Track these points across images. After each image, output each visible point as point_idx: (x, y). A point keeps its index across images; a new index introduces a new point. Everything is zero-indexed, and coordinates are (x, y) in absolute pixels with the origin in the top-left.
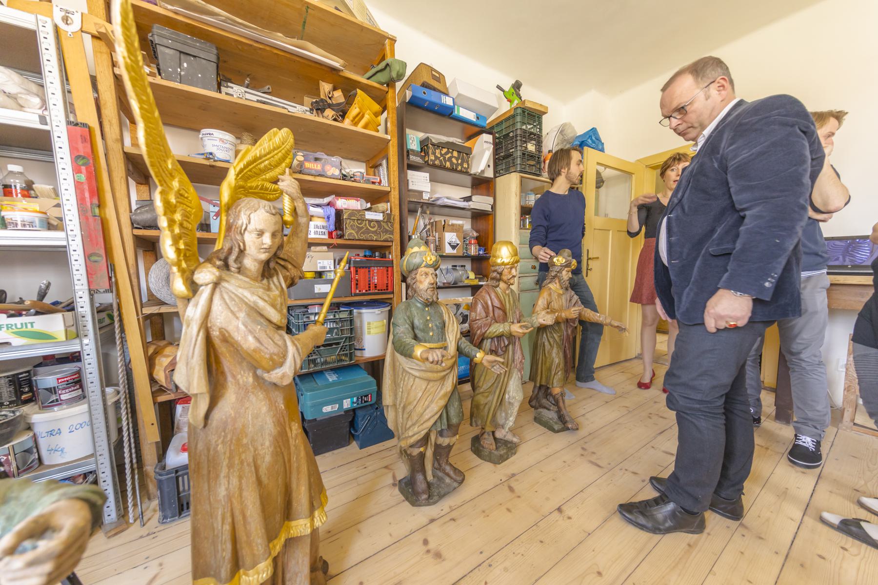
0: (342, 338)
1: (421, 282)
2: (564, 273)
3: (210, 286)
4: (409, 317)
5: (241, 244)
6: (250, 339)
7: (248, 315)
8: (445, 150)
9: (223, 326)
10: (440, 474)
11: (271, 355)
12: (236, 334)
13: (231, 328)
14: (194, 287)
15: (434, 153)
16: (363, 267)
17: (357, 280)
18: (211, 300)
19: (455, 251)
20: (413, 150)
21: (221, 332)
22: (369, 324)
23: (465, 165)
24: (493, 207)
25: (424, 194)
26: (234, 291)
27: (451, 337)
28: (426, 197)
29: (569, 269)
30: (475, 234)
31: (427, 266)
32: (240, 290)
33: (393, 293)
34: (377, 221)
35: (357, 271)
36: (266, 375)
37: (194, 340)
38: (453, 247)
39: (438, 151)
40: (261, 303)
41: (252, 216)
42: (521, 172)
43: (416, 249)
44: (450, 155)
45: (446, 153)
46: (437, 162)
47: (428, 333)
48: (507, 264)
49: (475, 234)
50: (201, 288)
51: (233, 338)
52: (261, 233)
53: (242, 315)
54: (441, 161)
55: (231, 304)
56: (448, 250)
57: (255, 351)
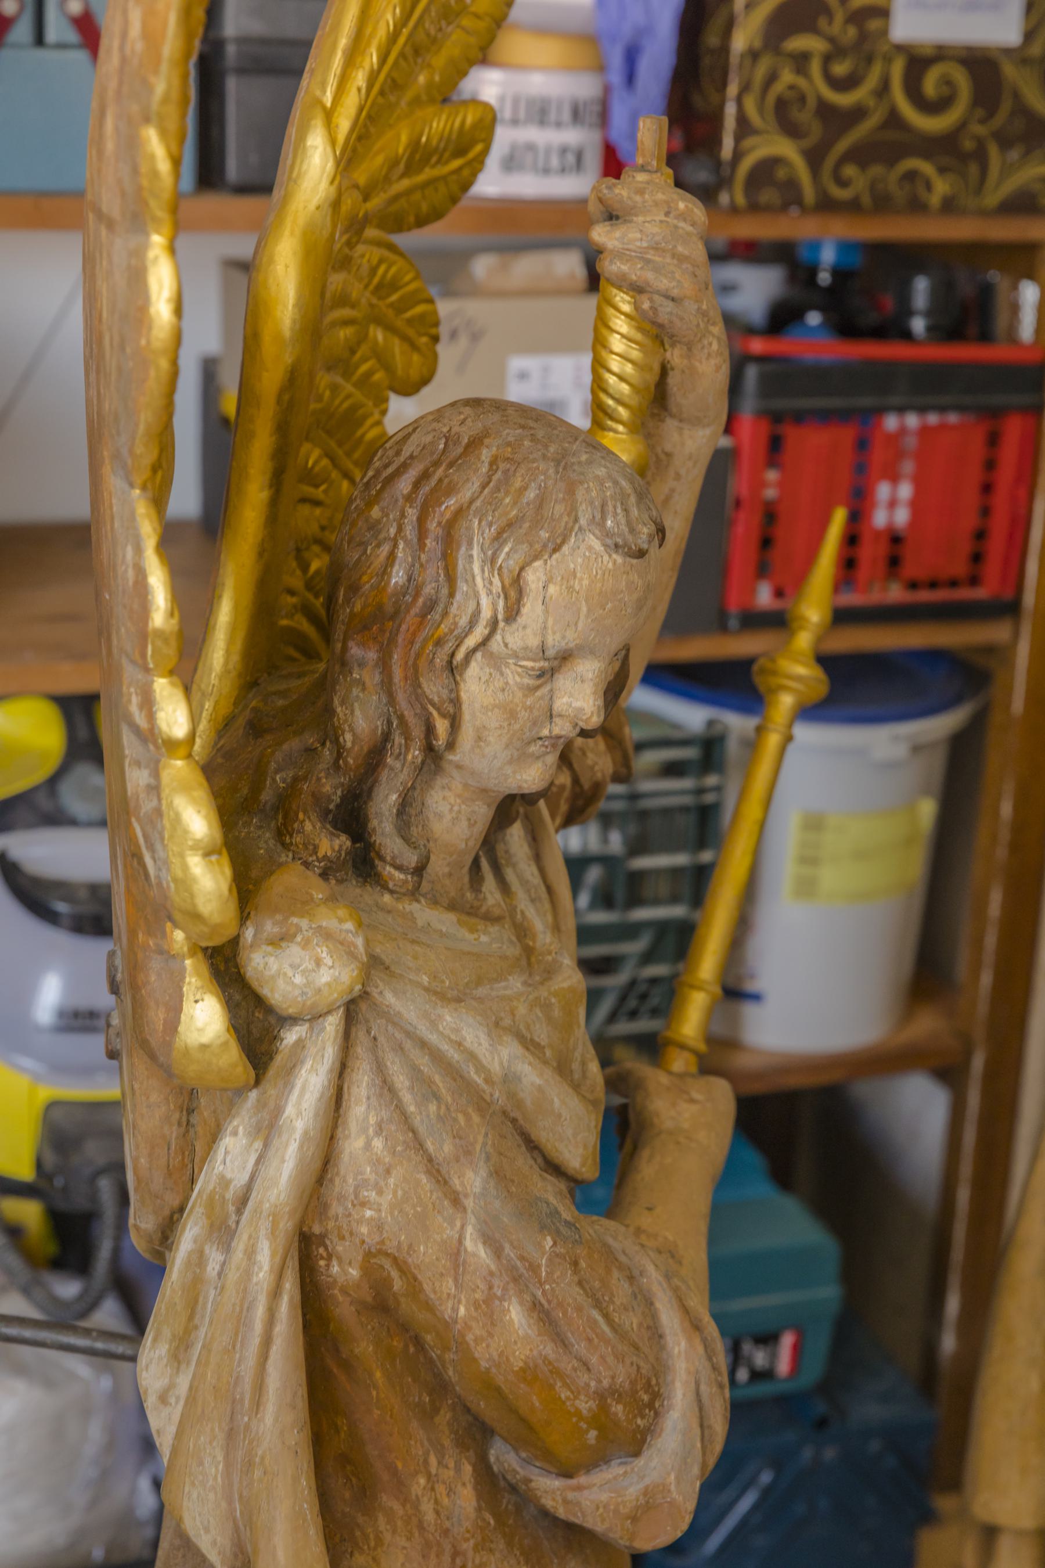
0: (631, 931)
3: (333, 1024)
5: (442, 726)
6: (516, 1314)
7: (498, 1174)
9: (391, 1247)
11: (601, 1397)
12: (448, 1285)
13: (425, 1255)
14: (258, 1030)
17: (770, 514)
18: (337, 1100)
21: (367, 1270)
22: (814, 824)
26: (423, 1030)
32: (448, 1018)
33: (1008, 608)
35: (775, 445)
36: (549, 1488)
37: (260, 1312)
40: (532, 1076)
41: (534, 577)
50: (291, 1036)
51: (428, 1307)
52: (554, 664)
53: (473, 1180)
55: (424, 1116)
57: (529, 1374)
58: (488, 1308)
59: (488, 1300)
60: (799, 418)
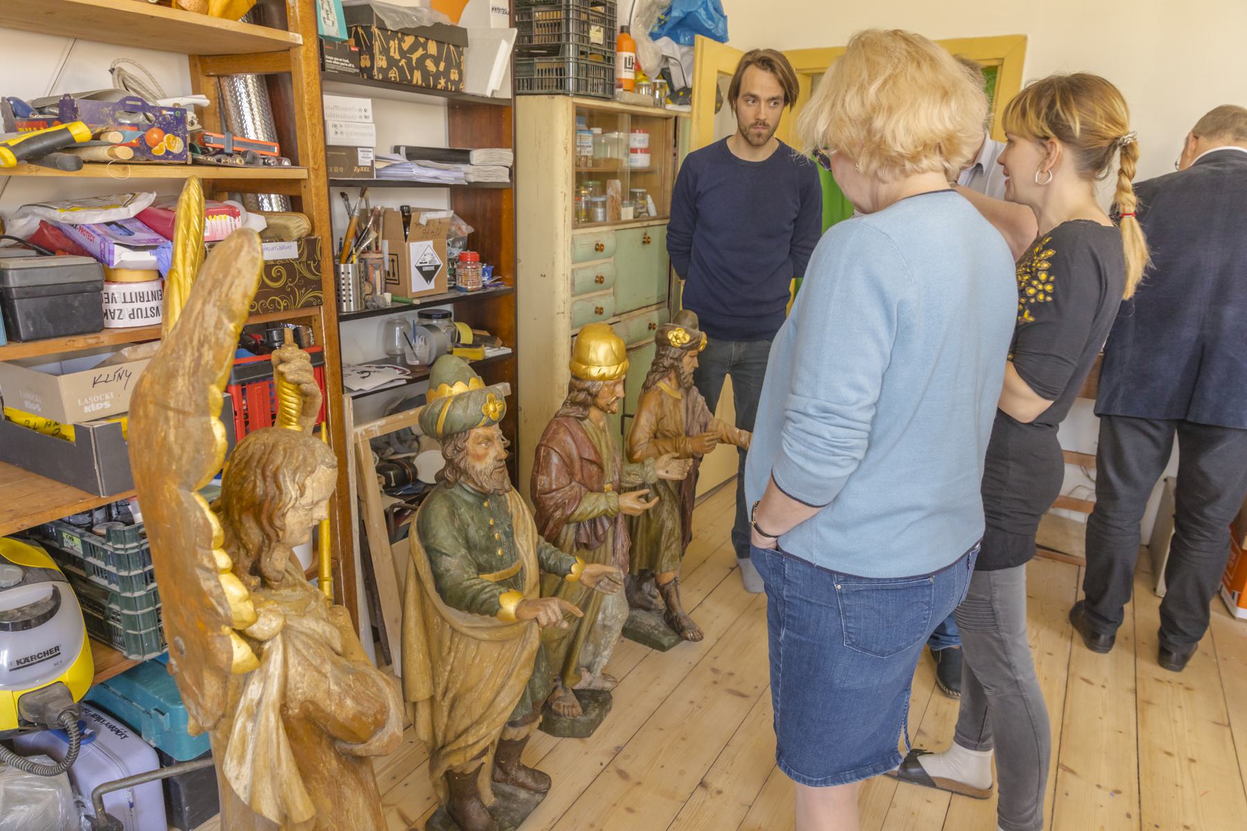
1: (479, 458)
2: (686, 359)
3: (279, 638)
4: (459, 530)
6: (349, 702)
8: (409, 41)
10: (508, 789)
12: (328, 702)
13: (320, 696)
15: (385, 51)
16: (257, 380)
19: (431, 286)
20: (330, 40)
23: (454, 76)
24: (513, 172)
25: (360, 154)
27: (524, 543)
28: (364, 159)
29: (695, 352)
30: (466, 229)
31: (489, 424)
34: (287, 264)
38: (428, 276)
39: (393, 44)
41: (308, 482)
42: (576, 95)
43: (459, 388)
44: (420, 52)
45: (413, 48)
46: (393, 74)
47: (494, 552)
48: (611, 378)
49: (466, 229)
52: (315, 504)
53: (328, 668)
54: (401, 69)
56: (418, 285)
58: (341, 704)
59: (341, 700)
60: (250, 382)
